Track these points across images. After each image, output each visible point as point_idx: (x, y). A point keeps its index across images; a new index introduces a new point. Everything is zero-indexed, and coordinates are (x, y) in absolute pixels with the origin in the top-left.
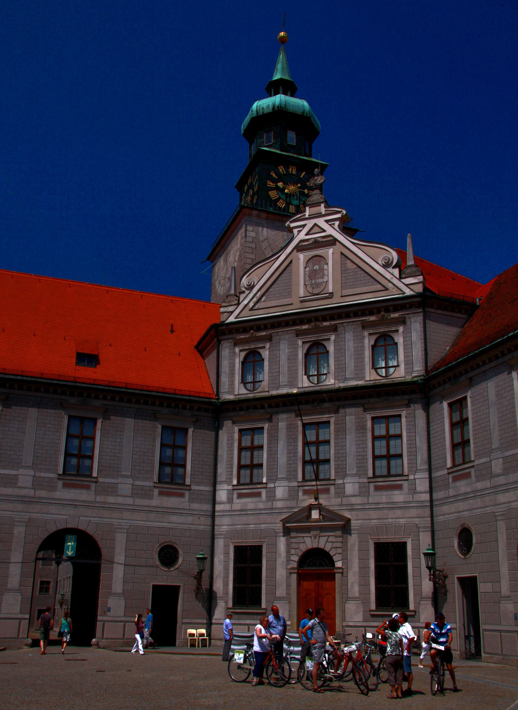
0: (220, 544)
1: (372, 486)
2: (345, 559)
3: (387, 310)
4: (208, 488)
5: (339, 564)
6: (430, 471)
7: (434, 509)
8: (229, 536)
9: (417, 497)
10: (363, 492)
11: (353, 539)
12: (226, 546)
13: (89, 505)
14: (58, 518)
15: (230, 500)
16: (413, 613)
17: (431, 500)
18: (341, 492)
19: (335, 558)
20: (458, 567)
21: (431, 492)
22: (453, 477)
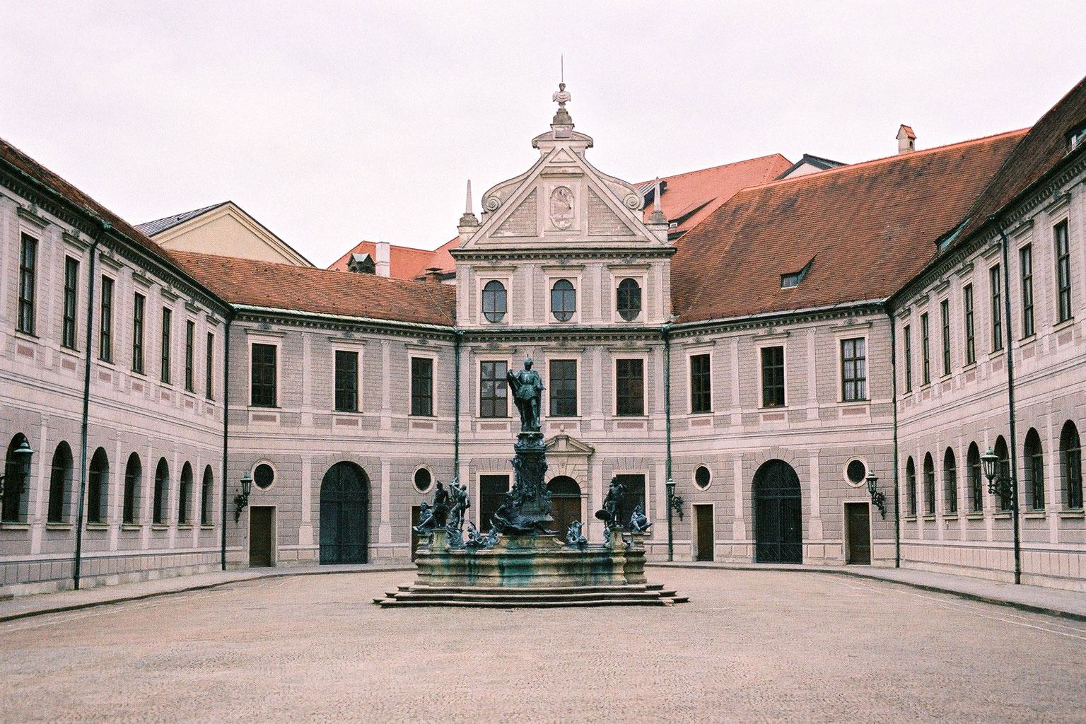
0: (464, 471)
1: (616, 423)
2: (589, 487)
3: (634, 255)
4: (454, 419)
5: (583, 491)
6: (668, 415)
7: (671, 445)
8: (473, 465)
9: (654, 434)
10: (608, 426)
11: (597, 470)
12: (472, 473)
13: (361, 440)
14: (336, 451)
15: (473, 430)
16: (649, 534)
17: (669, 438)
18: (585, 427)
19: (581, 486)
20: (696, 495)
21: (669, 430)
22: (693, 421)
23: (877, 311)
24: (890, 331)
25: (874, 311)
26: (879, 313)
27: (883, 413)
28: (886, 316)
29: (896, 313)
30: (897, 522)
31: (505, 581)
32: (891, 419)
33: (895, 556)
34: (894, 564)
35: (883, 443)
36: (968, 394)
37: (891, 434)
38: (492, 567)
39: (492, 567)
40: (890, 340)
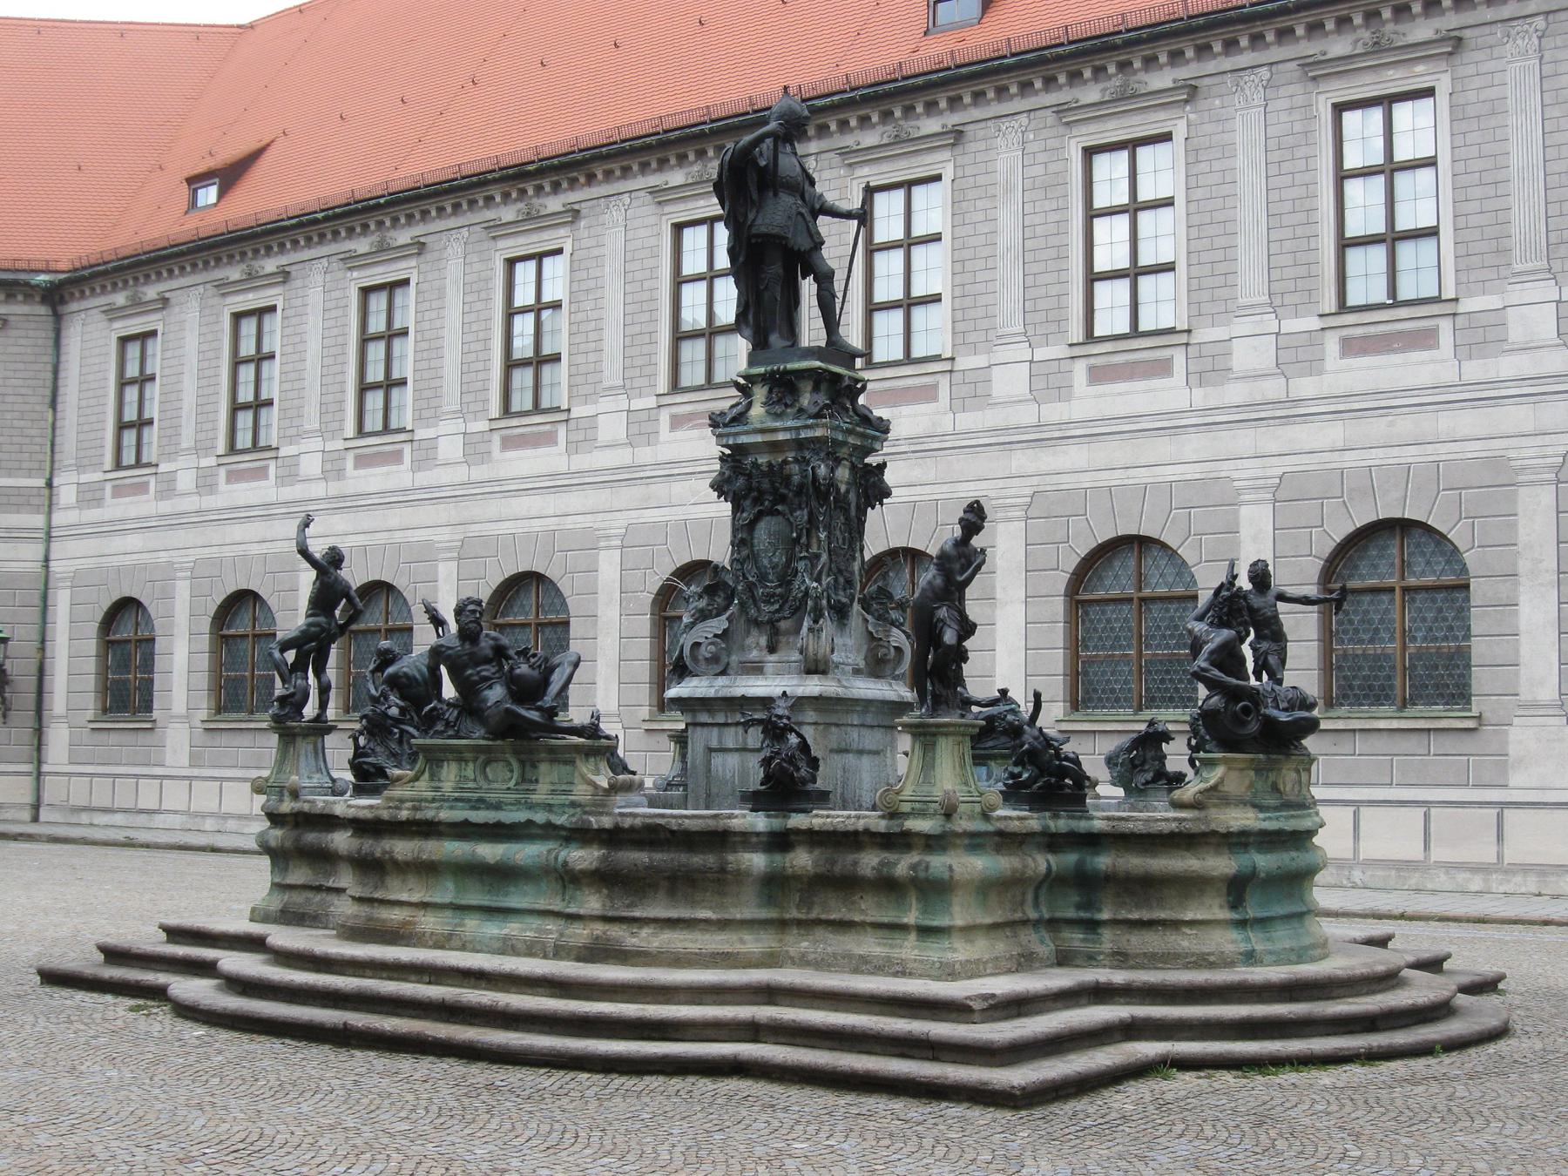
23: (20, 298)
24: (51, 342)
25: (14, 296)
26: (25, 302)
27: (18, 508)
28: (43, 310)
29: (74, 306)
30: (39, 732)
31: (1256, 941)
32: (38, 520)
33: (28, 799)
34: (26, 815)
35: (15, 567)
36: (502, 474)
37: (35, 551)
38: (1192, 885)
39: (1192, 885)
40: (48, 359)
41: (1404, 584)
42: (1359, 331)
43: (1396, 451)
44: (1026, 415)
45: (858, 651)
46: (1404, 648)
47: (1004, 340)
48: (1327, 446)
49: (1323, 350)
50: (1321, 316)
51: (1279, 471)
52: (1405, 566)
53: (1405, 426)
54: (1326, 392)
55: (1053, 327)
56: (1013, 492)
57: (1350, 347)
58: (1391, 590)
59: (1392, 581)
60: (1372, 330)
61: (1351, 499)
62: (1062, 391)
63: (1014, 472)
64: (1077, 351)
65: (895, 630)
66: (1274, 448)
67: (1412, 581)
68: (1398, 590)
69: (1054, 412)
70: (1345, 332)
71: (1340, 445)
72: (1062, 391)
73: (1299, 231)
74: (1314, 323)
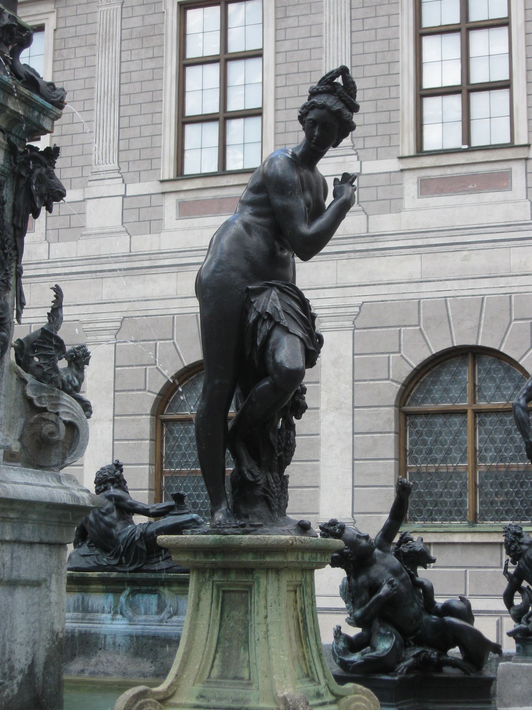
41: (475, 407)
42: (436, 173)
43: (470, 284)
44: (119, 245)
45: (10, 427)
46: (475, 467)
47: (99, 177)
48: (405, 279)
49: (402, 190)
50: (400, 158)
51: (359, 301)
52: (476, 390)
53: (479, 260)
54: (404, 228)
55: (146, 165)
56: (103, 317)
57: (427, 187)
58: (463, 413)
59: (464, 404)
60: (449, 172)
61: (427, 327)
62: (154, 225)
63: (105, 298)
64: (168, 187)
65: (66, 398)
66: (353, 279)
67: (483, 404)
68: (470, 414)
69: (145, 243)
70: (423, 174)
71: (417, 277)
72: (154, 225)
73: (381, 82)
74: (394, 165)
